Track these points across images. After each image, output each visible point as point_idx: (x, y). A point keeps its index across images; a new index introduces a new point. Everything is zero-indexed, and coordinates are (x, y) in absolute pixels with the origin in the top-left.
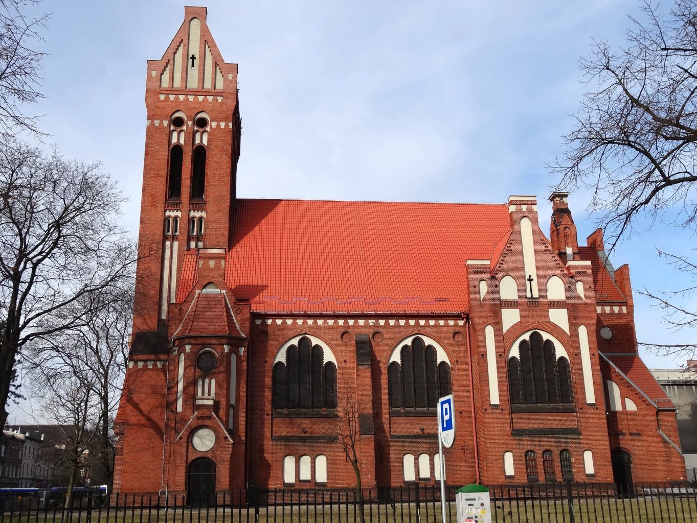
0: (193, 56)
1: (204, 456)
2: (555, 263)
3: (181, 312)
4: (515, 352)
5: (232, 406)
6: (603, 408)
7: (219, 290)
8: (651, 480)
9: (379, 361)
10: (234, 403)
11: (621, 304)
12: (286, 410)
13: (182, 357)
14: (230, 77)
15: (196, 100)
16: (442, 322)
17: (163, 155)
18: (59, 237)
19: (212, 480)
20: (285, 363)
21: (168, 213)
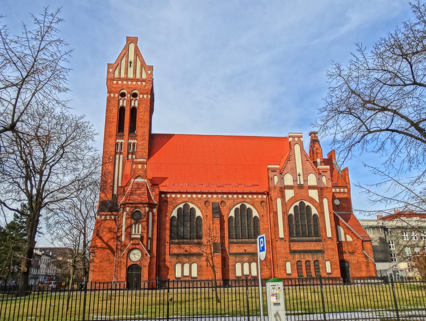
0: (131, 61)
1: (136, 263)
2: (312, 167)
3: (124, 191)
4: (291, 211)
5: (150, 238)
6: (335, 239)
7: (143, 180)
8: (359, 276)
9: (224, 216)
10: (151, 237)
11: (344, 187)
12: (177, 241)
13: (125, 213)
14: (149, 72)
16: (255, 196)
17: (115, 111)
18: (64, 153)
19: (139, 276)
20: (176, 217)
21: (117, 141)
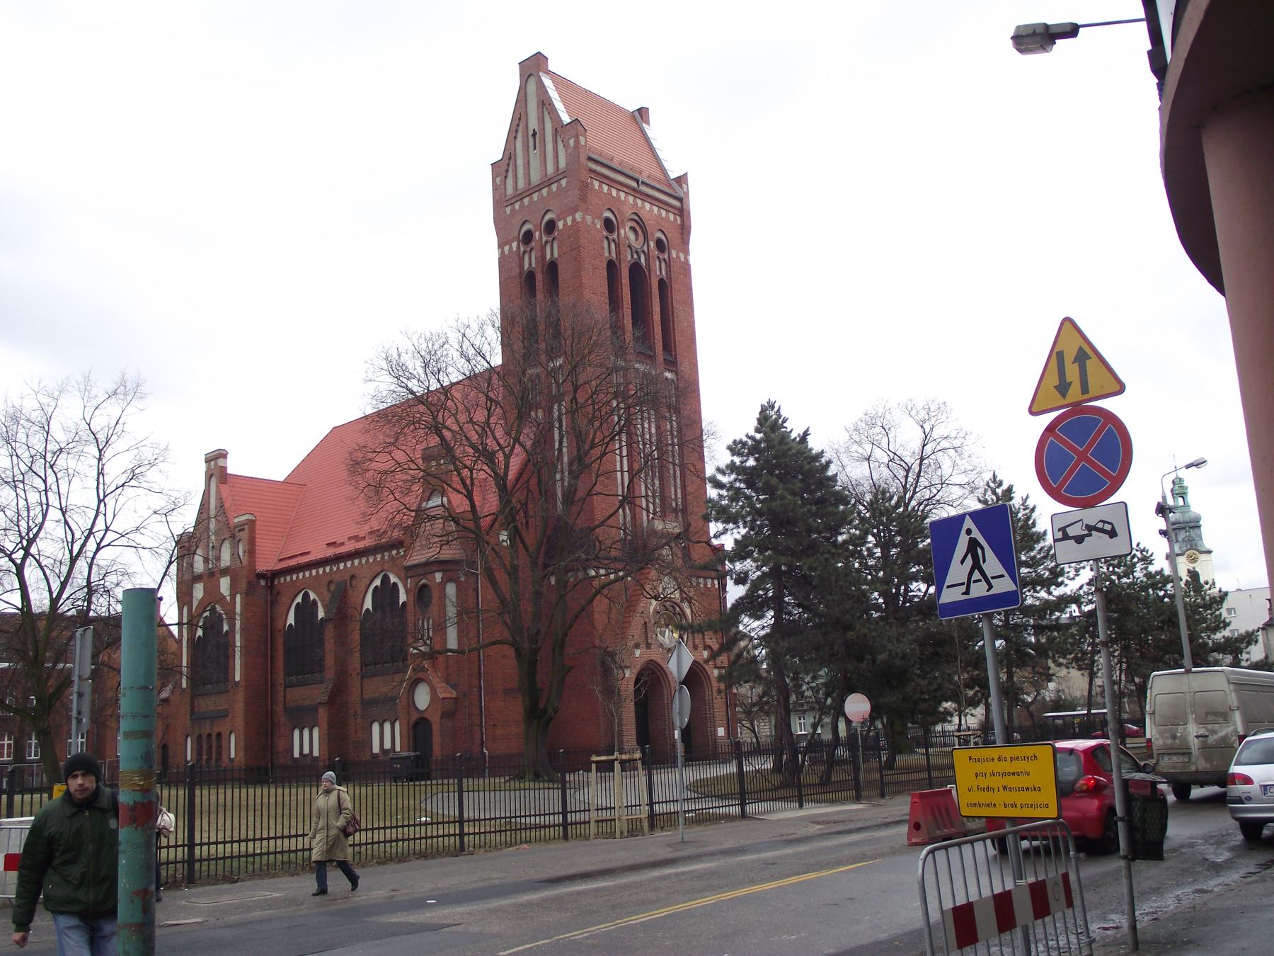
15: (541, 199)
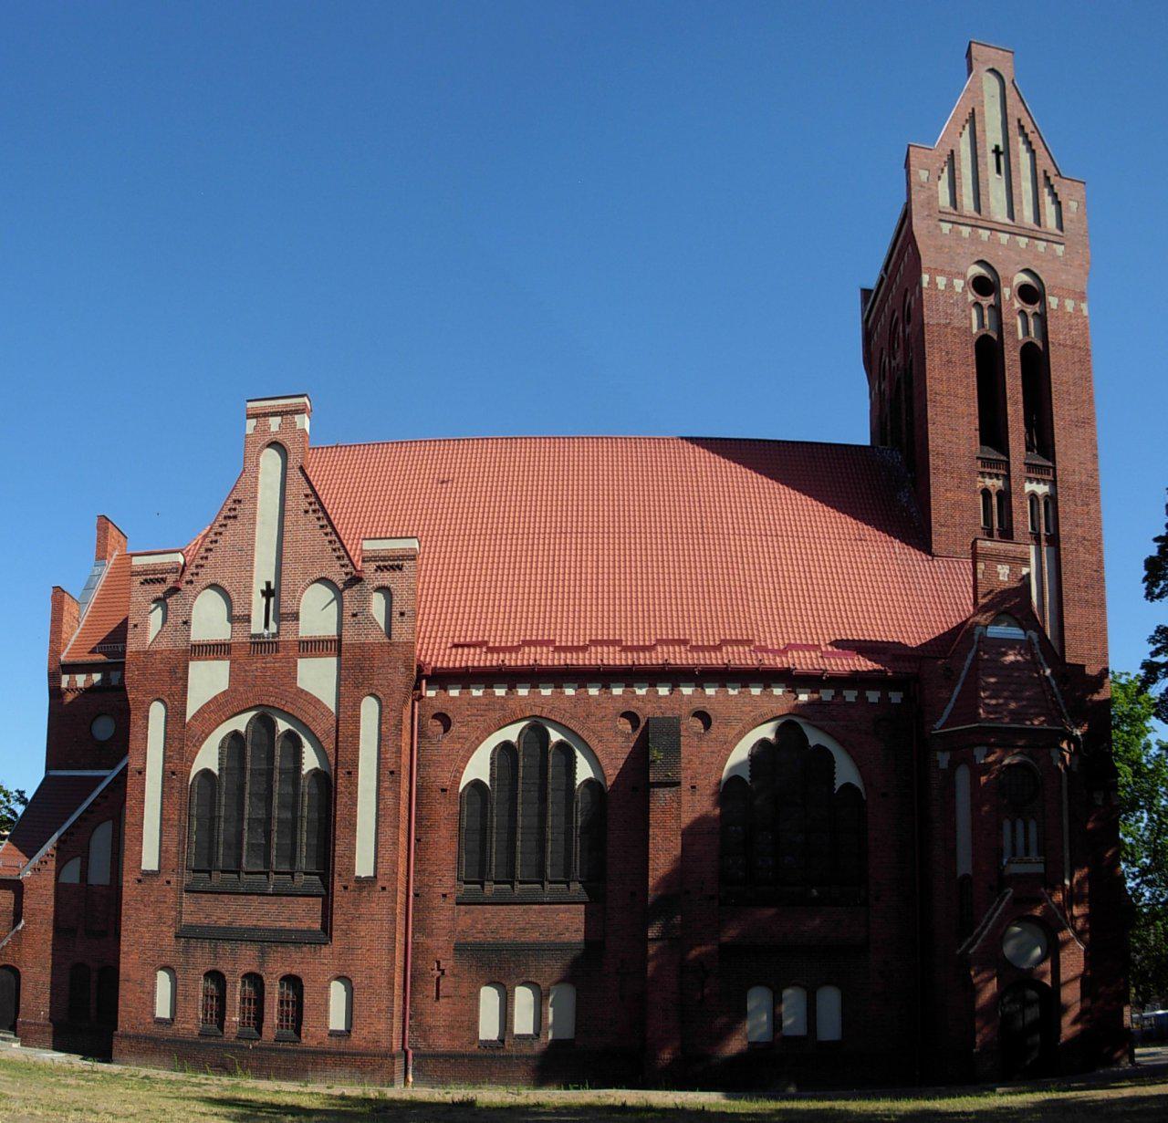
4: (208, 757)
